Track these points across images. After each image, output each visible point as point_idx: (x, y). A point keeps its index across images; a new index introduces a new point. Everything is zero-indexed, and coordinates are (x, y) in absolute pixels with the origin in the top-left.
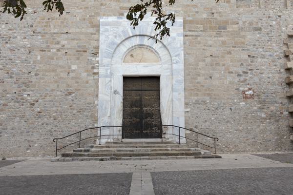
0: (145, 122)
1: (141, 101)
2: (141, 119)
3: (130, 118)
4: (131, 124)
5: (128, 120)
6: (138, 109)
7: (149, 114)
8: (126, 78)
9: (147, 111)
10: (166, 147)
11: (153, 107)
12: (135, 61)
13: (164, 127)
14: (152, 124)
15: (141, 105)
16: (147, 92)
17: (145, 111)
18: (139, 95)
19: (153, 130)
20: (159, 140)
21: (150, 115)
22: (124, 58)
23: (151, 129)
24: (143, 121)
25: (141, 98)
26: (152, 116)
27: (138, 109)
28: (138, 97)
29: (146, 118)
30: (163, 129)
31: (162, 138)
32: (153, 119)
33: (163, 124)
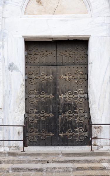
0: (62, 119)
1: (55, 83)
2: (57, 113)
3: (37, 113)
4: (38, 122)
5: (34, 115)
6: (51, 96)
7: (69, 104)
8: (31, 44)
9: (65, 101)
10: (99, 162)
11: (76, 93)
12: (46, 12)
13: (96, 128)
14: (75, 121)
15: (56, 89)
16: (65, 69)
17: (62, 101)
18: (53, 73)
19: (76, 132)
20: (86, 149)
21: (71, 107)
22: (25, 6)
23: (73, 131)
24: (60, 117)
25: (55, 78)
26: (75, 109)
27: (51, 96)
28: (51, 77)
29: (64, 112)
30: (94, 131)
31: (90, 144)
32: (76, 113)
33: (93, 123)
